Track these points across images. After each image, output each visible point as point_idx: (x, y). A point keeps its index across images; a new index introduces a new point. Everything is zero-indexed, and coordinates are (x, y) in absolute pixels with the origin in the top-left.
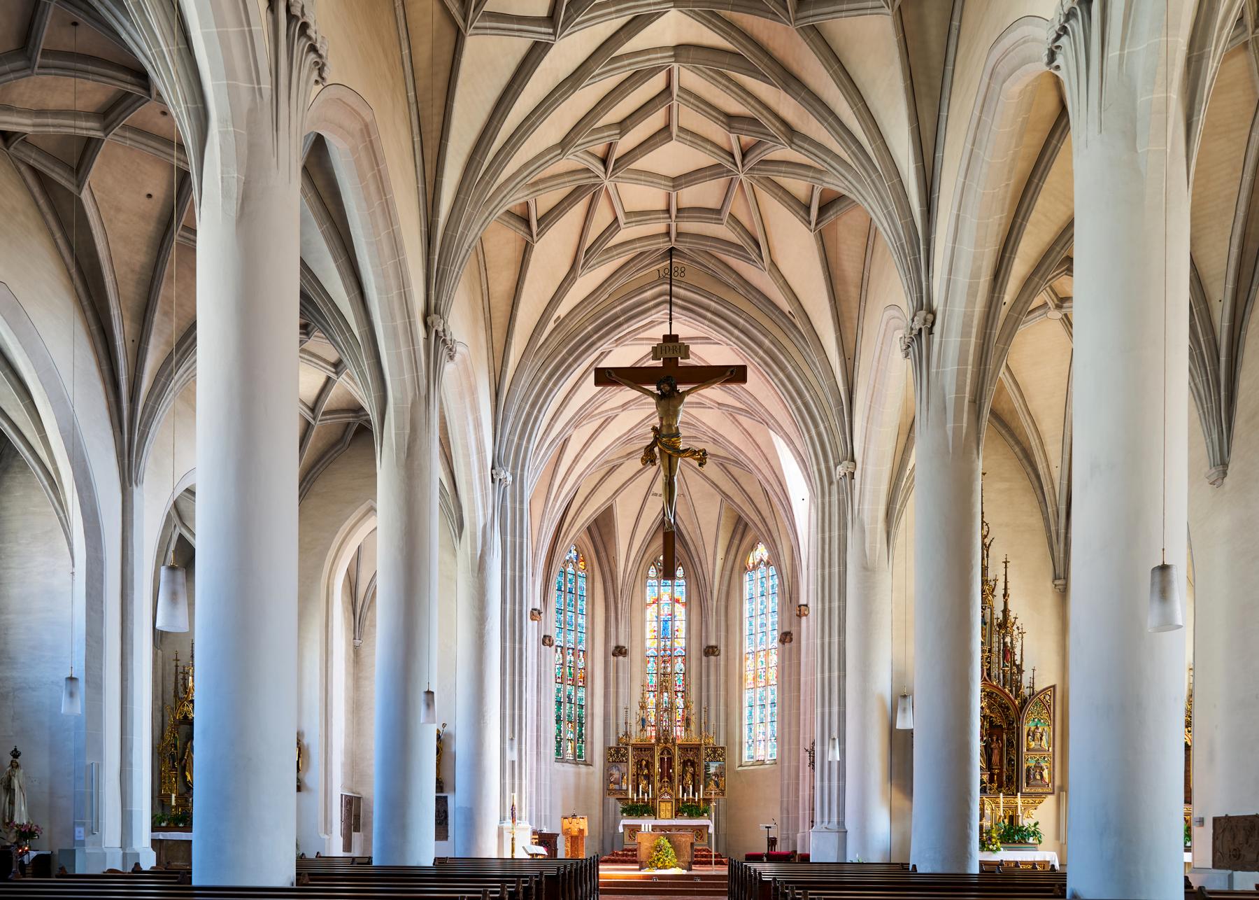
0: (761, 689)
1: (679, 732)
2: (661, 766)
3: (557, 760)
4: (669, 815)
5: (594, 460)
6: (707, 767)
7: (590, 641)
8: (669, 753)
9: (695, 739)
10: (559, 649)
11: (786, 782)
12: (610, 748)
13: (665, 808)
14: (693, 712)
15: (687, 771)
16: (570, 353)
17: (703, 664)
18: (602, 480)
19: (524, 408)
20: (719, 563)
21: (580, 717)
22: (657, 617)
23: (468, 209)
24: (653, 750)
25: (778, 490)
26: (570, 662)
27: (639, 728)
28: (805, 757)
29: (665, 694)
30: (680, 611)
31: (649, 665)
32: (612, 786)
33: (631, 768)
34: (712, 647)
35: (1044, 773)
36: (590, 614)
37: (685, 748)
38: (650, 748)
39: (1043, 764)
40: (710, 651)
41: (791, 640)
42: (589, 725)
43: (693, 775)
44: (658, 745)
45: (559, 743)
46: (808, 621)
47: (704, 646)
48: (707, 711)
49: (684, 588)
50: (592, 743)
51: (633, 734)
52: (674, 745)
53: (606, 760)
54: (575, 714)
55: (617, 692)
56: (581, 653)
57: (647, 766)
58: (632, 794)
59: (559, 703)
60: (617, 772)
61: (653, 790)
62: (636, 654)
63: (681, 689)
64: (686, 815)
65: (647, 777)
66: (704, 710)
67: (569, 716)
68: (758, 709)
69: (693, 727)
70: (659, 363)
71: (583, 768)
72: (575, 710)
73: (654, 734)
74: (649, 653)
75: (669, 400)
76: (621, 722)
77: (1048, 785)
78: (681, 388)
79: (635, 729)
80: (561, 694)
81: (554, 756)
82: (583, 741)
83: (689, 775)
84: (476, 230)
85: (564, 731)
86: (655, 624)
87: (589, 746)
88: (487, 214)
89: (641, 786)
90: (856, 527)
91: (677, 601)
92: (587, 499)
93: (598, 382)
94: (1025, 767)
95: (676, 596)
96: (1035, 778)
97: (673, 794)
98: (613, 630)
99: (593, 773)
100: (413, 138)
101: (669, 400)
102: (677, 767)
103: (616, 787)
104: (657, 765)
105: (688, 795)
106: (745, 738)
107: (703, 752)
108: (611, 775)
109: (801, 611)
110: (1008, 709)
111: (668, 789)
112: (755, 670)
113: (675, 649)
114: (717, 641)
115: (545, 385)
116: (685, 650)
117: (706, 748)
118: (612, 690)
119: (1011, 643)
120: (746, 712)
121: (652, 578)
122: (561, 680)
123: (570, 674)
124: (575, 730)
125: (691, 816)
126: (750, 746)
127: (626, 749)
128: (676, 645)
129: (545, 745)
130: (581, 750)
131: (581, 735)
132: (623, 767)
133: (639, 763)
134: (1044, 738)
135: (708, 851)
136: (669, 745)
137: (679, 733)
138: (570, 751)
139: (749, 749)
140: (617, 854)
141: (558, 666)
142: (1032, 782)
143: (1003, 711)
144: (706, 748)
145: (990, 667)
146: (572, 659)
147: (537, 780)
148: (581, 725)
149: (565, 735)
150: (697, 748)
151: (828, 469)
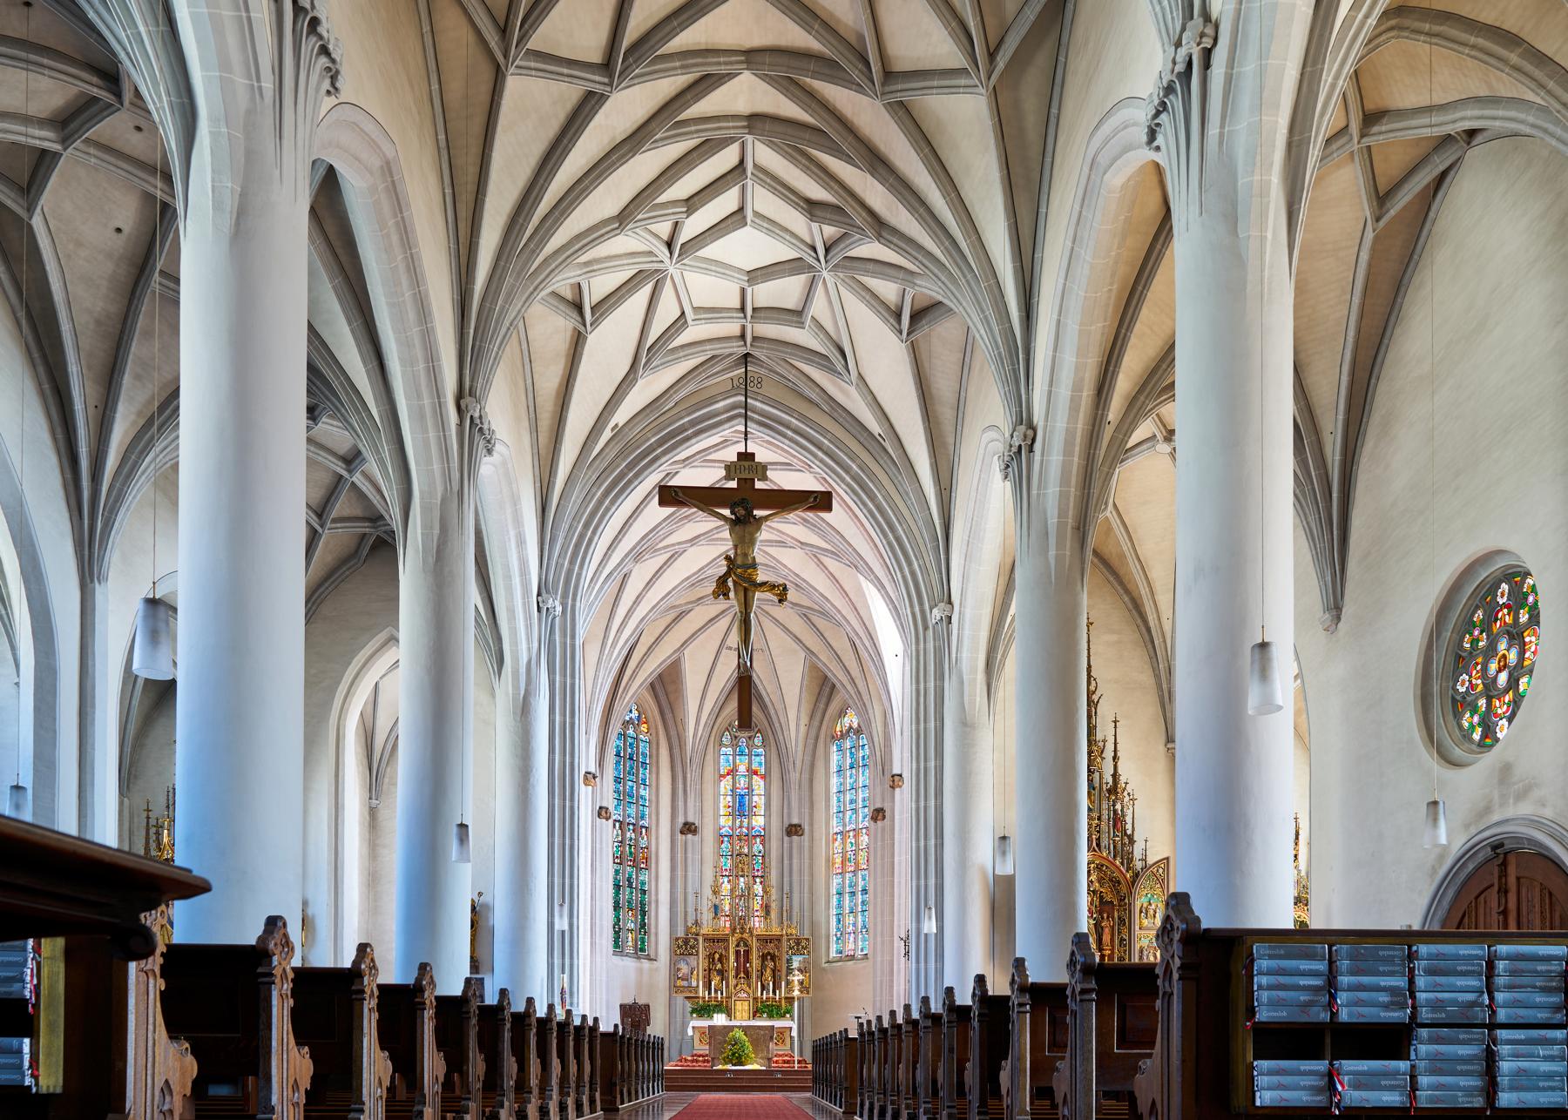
0: (851, 875)
1: (757, 924)
2: (737, 960)
3: (615, 953)
4: (746, 1015)
5: (658, 603)
6: (789, 961)
7: (654, 817)
8: (746, 945)
9: (776, 931)
10: (617, 825)
11: (879, 979)
12: (677, 939)
13: (742, 1008)
14: (773, 897)
15: (766, 966)
16: (630, 467)
17: (785, 845)
18: (668, 628)
19: (577, 527)
20: (803, 729)
21: (643, 904)
22: (732, 791)
23: (509, 281)
24: (727, 941)
25: (867, 644)
26: (631, 839)
27: (712, 915)
28: (899, 948)
29: (742, 879)
30: (758, 783)
31: (723, 846)
32: (679, 983)
33: (700, 962)
34: (795, 825)
36: (654, 784)
37: (764, 940)
38: (723, 940)
40: (793, 830)
41: (884, 817)
42: (653, 914)
43: (774, 971)
44: (733, 935)
45: (617, 934)
46: (902, 793)
47: (786, 825)
48: (790, 898)
49: (763, 758)
50: (656, 934)
51: (705, 922)
52: (752, 935)
53: (673, 953)
54: (636, 900)
55: (686, 876)
56: (644, 830)
57: (720, 960)
58: (704, 991)
59: (617, 887)
60: (686, 967)
61: (727, 987)
62: (708, 833)
63: (760, 874)
64: (765, 1015)
65: (721, 973)
66: (786, 894)
67: (629, 902)
68: (847, 897)
69: (773, 915)
70: (733, 484)
71: (646, 964)
72: (637, 894)
73: (728, 925)
74: (723, 831)
75: (744, 524)
76: (691, 910)
78: (758, 513)
79: (707, 916)
80: (620, 877)
81: (611, 949)
82: (645, 932)
83: (768, 971)
84: (519, 306)
85: (624, 920)
86: (729, 798)
87: (653, 938)
88: (531, 289)
89: (713, 983)
90: (954, 677)
91: (755, 773)
92: (650, 649)
93: (662, 503)
95: (754, 767)
97: (751, 992)
98: (681, 804)
99: (657, 970)
100: (444, 189)
101: (744, 524)
102: (755, 962)
103: (685, 983)
104: (732, 958)
105: (768, 993)
106: (833, 930)
107: (785, 943)
108: (679, 970)
109: (895, 781)
110: (1119, 882)
111: (745, 987)
112: (844, 853)
113: (753, 828)
114: (800, 818)
115: (600, 502)
116: (764, 829)
117: (789, 940)
118: (679, 873)
119: (1122, 810)
120: (834, 900)
121: (726, 746)
122: (619, 860)
123: (631, 853)
124: (636, 918)
125: (771, 1017)
126: (838, 939)
127: (696, 940)
128: (754, 823)
129: (601, 935)
130: (643, 942)
131: (643, 925)
132: (693, 961)
133: (711, 957)
135: (791, 1056)
136: (746, 936)
137: (757, 925)
138: (630, 944)
139: (837, 943)
140: (686, 1060)
141: (616, 844)
144: (789, 940)
146: (633, 836)
147: (591, 975)
148: (644, 913)
149: (625, 924)
150: (779, 939)
151: (923, 612)
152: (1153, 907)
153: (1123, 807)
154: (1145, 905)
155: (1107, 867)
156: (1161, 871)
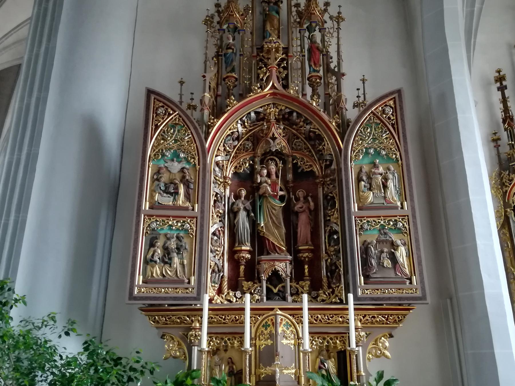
35: (398, 254)
39: (395, 237)
77: (410, 279)
94: (357, 242)
96: (380, 264)
110: (320, 138)
119: (323, 40)
134: (391, 184)
142: (376, 273)
143: (313, 146)
145: (287, 75)
152: (381, 170)
153: (323, 36)
154: (366, 169)
155: (299, 115)
156: (389, 111)
